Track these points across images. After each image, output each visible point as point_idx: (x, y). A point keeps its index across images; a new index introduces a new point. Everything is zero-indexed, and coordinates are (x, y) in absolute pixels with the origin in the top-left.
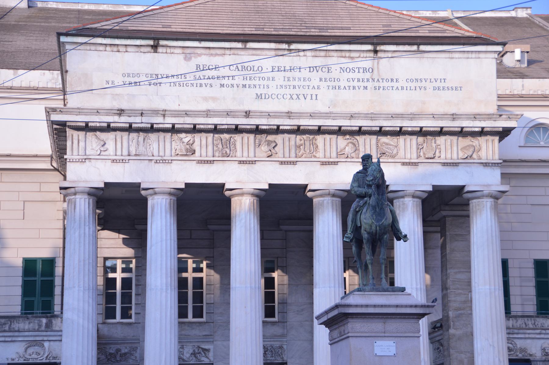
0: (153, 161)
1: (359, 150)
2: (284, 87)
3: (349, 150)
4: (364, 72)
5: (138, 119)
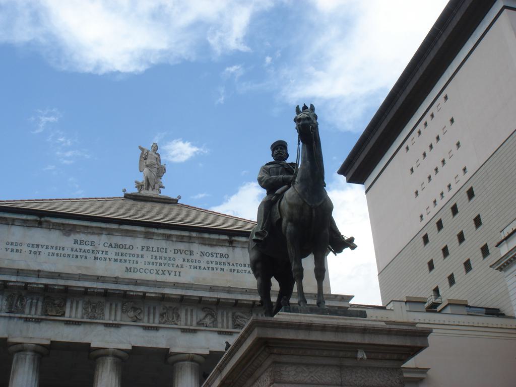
1: (217, 320)
2: (151, 264)
3: (208, 321)
4: (221, 257)
5: (13, 278)
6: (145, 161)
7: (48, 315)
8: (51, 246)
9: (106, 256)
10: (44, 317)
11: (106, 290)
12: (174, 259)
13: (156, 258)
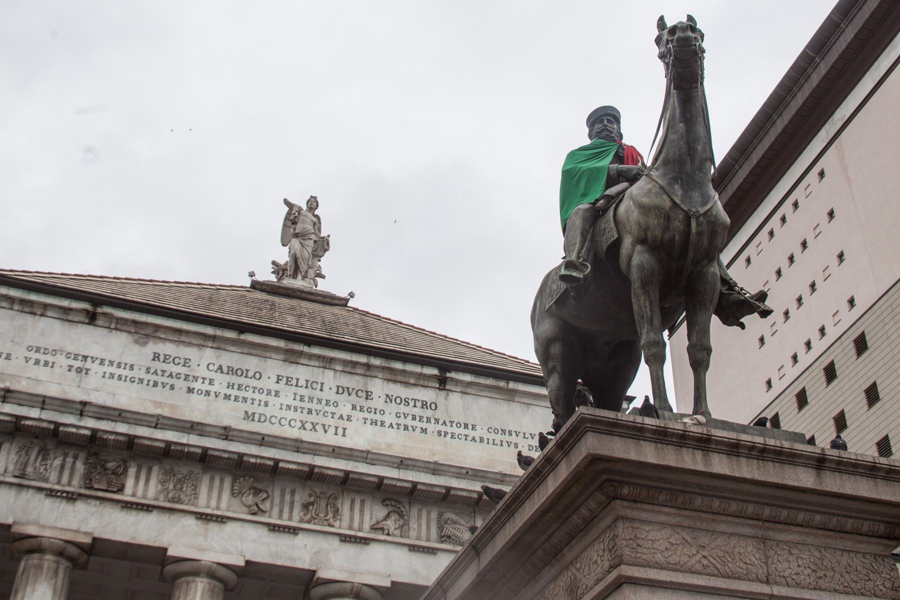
0: (44, 493)
2: (292, 409)
3: (391, 524)
4: (422, 407)
5: (34, 413)
6: (293, 226)
7: (91, 488)
8: (110, 361)
9: (209, 388)
10: (83, 491)
11: (205, 450)
12: (336, 404)
13: (302, 400)
